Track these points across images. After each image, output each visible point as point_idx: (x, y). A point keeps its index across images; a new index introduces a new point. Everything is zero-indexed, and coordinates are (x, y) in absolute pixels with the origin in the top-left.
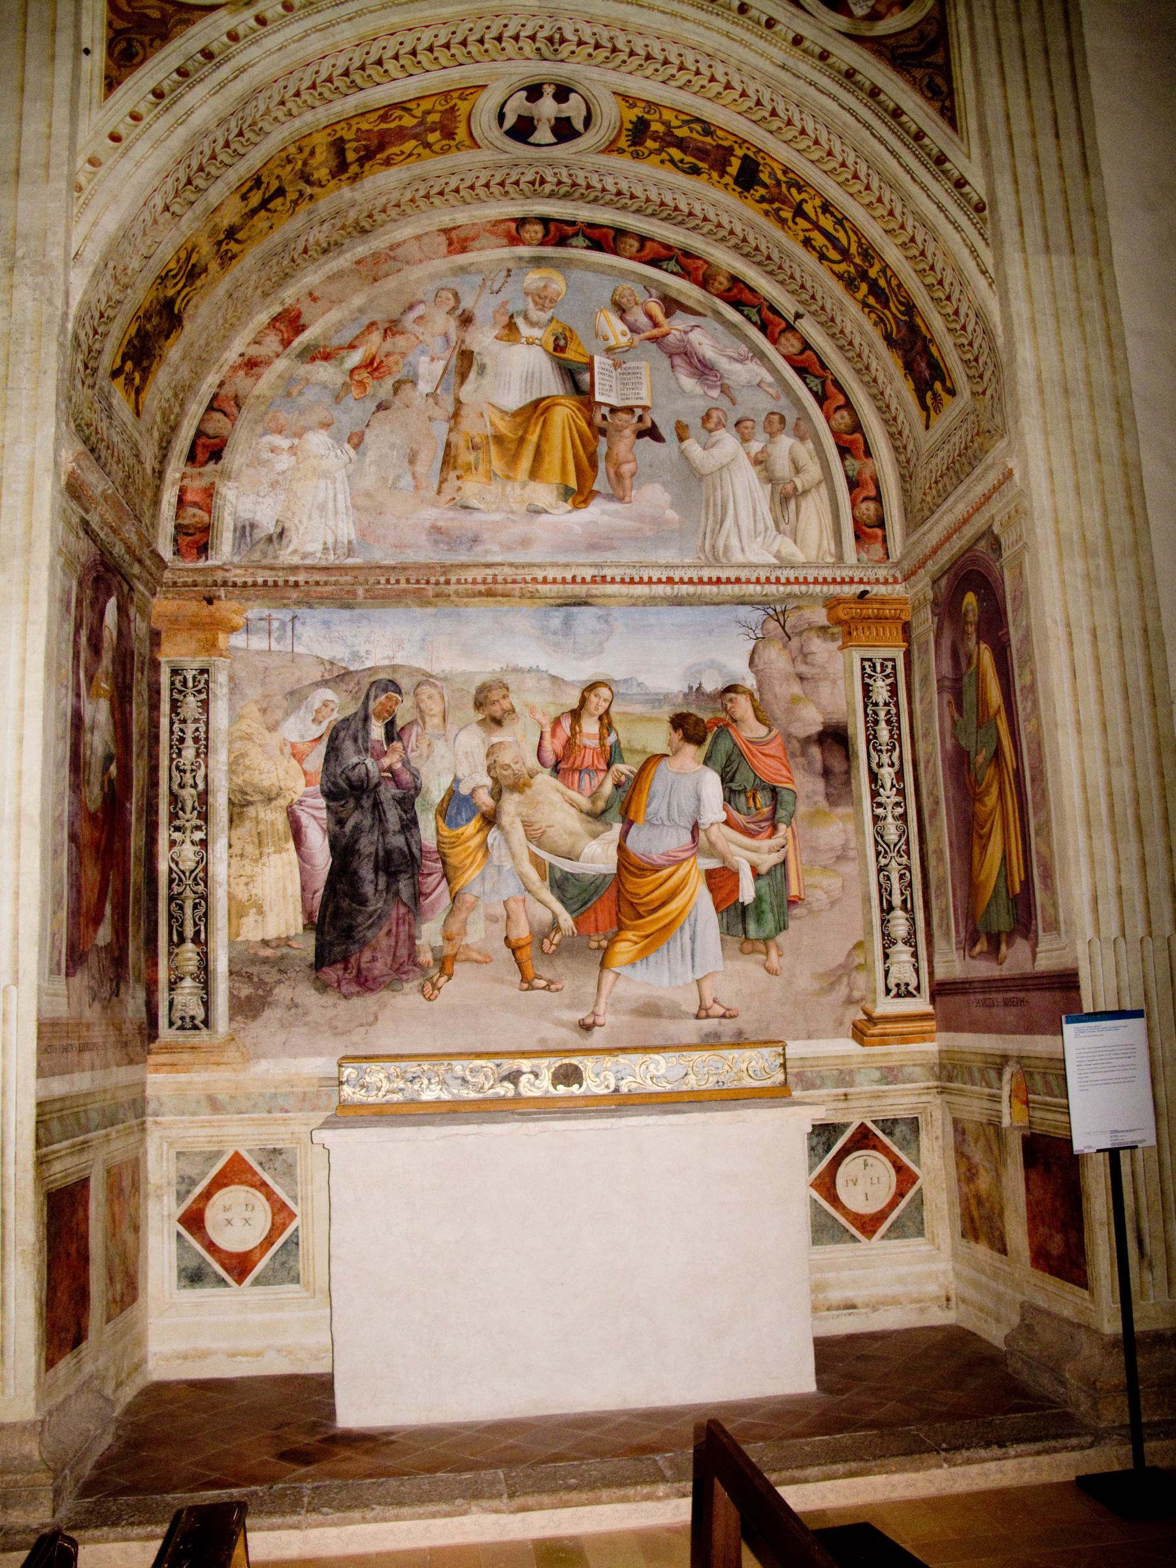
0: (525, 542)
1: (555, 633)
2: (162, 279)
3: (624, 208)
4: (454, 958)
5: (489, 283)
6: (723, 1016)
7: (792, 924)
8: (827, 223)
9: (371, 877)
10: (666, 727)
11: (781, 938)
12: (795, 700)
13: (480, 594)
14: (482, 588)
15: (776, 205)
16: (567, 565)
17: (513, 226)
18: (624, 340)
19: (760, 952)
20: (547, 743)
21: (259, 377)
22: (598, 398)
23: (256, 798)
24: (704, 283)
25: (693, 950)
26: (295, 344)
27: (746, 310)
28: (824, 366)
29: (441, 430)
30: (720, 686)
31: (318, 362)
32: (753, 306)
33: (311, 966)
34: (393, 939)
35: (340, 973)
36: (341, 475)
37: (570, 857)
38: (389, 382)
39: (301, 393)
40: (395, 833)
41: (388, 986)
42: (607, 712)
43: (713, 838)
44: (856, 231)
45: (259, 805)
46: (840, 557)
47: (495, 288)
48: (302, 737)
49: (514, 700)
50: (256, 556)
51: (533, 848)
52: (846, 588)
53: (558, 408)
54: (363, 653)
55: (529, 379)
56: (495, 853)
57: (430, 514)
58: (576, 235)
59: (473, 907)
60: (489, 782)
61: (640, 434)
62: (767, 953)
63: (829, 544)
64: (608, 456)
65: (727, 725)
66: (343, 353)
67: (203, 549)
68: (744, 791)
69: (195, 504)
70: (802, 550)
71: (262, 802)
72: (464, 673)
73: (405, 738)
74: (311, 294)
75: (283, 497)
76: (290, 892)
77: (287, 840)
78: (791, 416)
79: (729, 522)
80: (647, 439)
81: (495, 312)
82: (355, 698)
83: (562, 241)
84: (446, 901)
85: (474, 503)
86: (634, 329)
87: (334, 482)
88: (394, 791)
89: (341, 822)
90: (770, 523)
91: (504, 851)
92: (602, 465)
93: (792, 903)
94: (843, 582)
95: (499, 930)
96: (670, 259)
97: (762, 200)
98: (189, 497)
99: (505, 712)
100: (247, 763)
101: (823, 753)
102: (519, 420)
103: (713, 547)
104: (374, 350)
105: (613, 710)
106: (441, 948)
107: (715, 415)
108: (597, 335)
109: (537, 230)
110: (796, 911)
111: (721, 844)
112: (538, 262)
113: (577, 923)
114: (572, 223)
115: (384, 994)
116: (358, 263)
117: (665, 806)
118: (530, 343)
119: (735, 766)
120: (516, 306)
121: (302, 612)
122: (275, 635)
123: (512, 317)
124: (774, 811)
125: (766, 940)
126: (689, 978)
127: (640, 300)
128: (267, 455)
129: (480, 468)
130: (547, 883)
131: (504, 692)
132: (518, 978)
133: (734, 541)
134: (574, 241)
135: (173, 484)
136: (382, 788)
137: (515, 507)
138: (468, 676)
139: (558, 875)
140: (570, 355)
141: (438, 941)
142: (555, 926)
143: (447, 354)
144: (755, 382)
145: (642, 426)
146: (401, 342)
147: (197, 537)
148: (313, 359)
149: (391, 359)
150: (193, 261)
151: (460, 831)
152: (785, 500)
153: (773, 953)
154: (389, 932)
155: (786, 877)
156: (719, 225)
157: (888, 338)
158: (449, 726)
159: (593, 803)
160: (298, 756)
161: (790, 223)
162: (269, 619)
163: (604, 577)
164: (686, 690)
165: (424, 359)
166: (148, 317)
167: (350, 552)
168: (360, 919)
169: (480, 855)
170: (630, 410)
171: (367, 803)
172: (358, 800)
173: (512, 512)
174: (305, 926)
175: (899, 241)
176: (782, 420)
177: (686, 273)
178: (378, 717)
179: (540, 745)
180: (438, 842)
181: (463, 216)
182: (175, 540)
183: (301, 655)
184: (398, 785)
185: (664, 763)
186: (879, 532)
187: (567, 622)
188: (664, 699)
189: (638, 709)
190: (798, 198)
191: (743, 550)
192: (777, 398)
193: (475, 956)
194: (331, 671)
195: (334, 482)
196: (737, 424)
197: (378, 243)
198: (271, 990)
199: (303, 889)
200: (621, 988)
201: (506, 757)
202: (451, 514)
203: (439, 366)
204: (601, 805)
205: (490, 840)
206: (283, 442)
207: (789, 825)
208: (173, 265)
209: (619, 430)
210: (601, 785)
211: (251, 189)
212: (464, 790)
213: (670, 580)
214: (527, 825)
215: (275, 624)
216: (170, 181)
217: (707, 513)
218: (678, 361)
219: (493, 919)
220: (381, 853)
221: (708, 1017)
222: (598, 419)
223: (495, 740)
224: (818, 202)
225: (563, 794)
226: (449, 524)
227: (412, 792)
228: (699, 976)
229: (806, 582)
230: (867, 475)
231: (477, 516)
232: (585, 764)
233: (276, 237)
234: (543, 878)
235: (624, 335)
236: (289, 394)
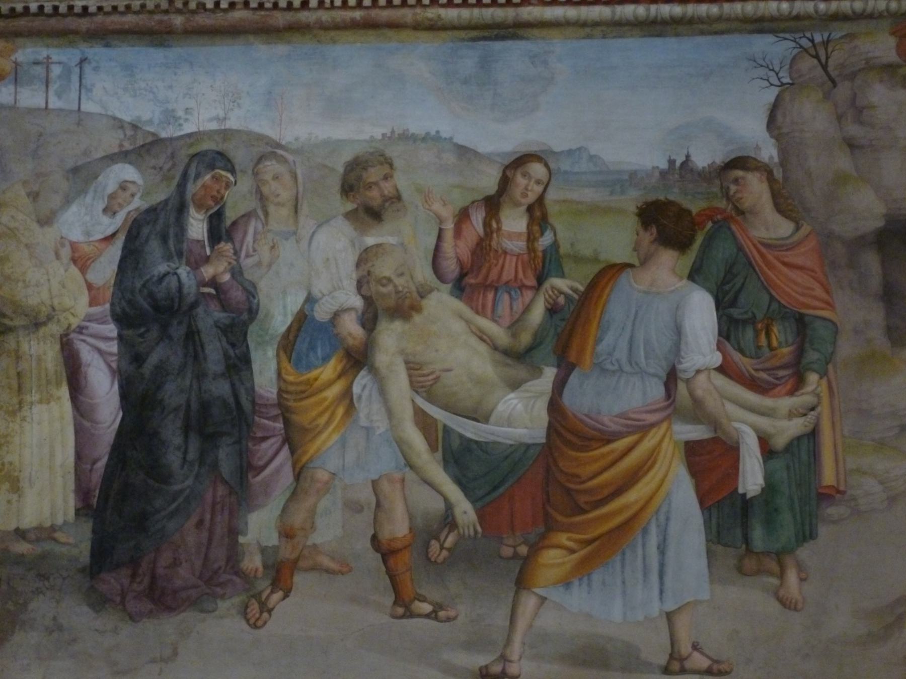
1: (465, 82)
4: (294, 565)
6: (709, 672)
7: (823, 531)
9: (178, 440)
10: (632, 222)
11: (804, 553)
12: (841, 179)
14: (358, 14)
19: (771, 574)
20: (448, 245)
23: (18, 322)
25: (662, 566)
30: (719, 159)
33: (82, 570)
34: (205, 534)
35: (126, 582)
37: (479, 415)
40: (216, 377)
41: (195, 603)
42: (541, 199)
43: (699, 393)
45: (21, 333)
48: (88, 234)
49: (401, 182)
51: (421, 403)
54: (180, 113)
56: (363, 410)
59: (327, 488)
60: (357, 302)
62: (782, 575)
65: (728, 219)
68: (753, 321)
71: (25, 327)
72: (327, 143)
73: (238, 236)
76: (59, 460)
77: (58, 385)
82: (167, 178)
84: (287, 478)
88: (219, 315)
89: (138, 359)
91: (377, 406)
93: (827, 496)
95: (363, 523)
99: (386, 199)
100: (8, 271)
101: (883, 263)
105: (552, 195)
106: (276, 549)
110: (832, 511)
111: (712, 403)
113: (481, 515)
115: (189, 616)
117: (623, 345)
119: (738, 282)
121: (96, 52)
122: (53, 88)
124: (800, 353)
125: (780, 556)
126: (655, 609)
130: (439, 455)
131: (386, 169)
132: (389, 599)
136: (200, 310)
138: (333, 146)
139: (456, 443)
141: (272, 539)
142: (448, 520)
151: (314, 373)
153: (792, 576)
154: (200, 524)
155: (815, 455)
158: (302, 219)
159: (514, 336)
160: (81, 261)
162: (47, 63)
164: (664, 165)
168: (158, 503)
169: (341, 411)
171: (178, 331)
172: (165, 327)
174: (78, 512)
178: (199, 207)
179: (437, 249)
180: (280, 391)
183: (89, 114)
184: (224, 307)
185: (625, 278)
187: (485, 64)
188: (633, 178)
189: (589, 195)
193: (326, 562)
194: (133, 138)
198: (25, 604)
199: (79, 456)
200: (548, 620)
201: (385, 268)
204: (526, 339)
205: (356, 389)
207: (823, 374)
210: (527, 309)
212: (322, 313)
214: (413, 367)
215: (56, 70)
219: (353, 507)
220: (194, 406)
221: (683, 671)
223: (370, 241)
225: (468, 322)
227: (245, 316)
228: (670, 606)
232: (505, 278)
234: (433, 448)
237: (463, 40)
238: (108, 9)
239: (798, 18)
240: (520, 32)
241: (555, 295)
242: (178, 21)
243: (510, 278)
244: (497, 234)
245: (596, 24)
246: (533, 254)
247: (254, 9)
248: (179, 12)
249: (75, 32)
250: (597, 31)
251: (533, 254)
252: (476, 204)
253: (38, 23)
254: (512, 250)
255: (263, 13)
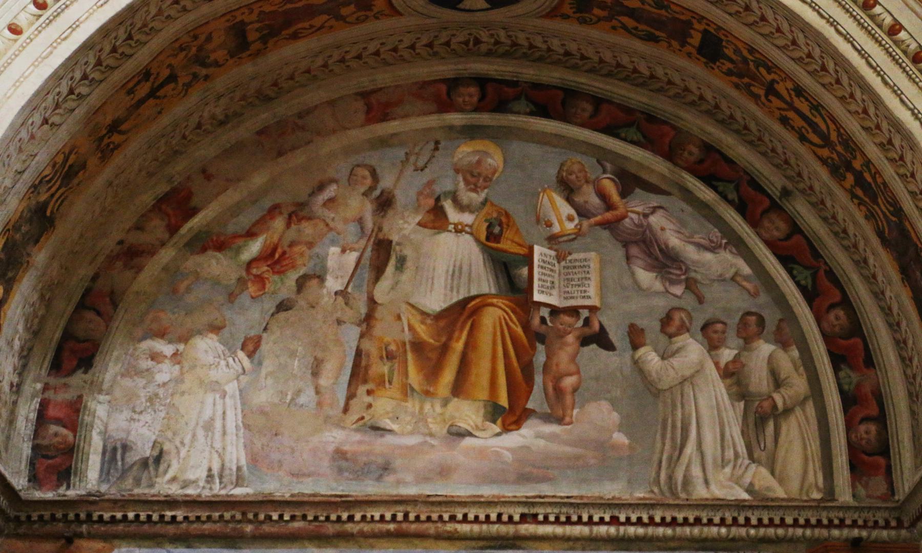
0: (444, 472)
2: (34, 188)
3: (575, 67)
5: (412, 159)
8: (804, 107)
13: (388, 535)
14: (392, 527)
15: (746, 80)
16: (490, 503)
17: (443, 88)
18: (570, 226)
21: (140, 269)
22: (537, 297)
24: (669, 155)
26: (184, 230)
27: (721, 186)
28: (816, 254)
29: (352, 334)
31: (210, 253)
32: (730, 182)
36: (232, 388)
38: (292, 277)
39: (188, 290)
44: (834, 120)
46: (830, 492)
47: (420, 164)
50: (129, 483)
52: (836, 533)
53: (491, 309)
55: (457, 273)
57: (335, 437)
58: (517, 98)
61: (585, 341)
63: (816, 477)
64: (546, 368)
66: (240, 242)
67: (65, 475)
69: (58, 421)
70: (781, 481)
74: (204, 171)
75: (163, 414)
78: (772, 316)
79: (690, 448)
80: (594, 346)
81: (420, 194)
83: (501, 107)
85: (387, 423)
86: (583, 212)
87: (224, 396)
90: (742, 449)
92: (538, 379)
94: (831, 525)
96: (629, 125)
97: (729, 73)
98: (52, 412)
102: (442, 323)
103: (670, 478)
104: (275, 239)
107: (677, 317)
108: (538, 221)
109: (471, 93)
112: (471, 132)
114: (514, 84)
116: (260, 133)
118: (459, 230)
120: (446, 185)
123: (438, 199)
127: (592, 177)
128: (146, 364)
129: (395, 380)
133: (696, 471)
134: (516, 106)
135: (33, 397)
137: (434, 427)
140: (505, 245)
143: (363, 242)
144: (729, 275)
145: (587, 331)
146: (308, 229)
147: (58, 460)
148: (204, 250)
149: (296, 249)
150: (70, 162)
152: (761, 421)
156: (686, 89)
157: (880, 234)
161: (763, 98)
163: (535, 516)
165: (334, 250)
166: (16, 228)
167: (239, 481)
170: (574, 311)
173: (431, 435)
175: (878, 140)
176: (761, 321)
177: (647, 143)
181: (384, 78)
182: (32, 463)
186: (881, 461)
190: (769, 78)
191: (706, 482)
192: (755, 295)
195: (224, 396)
196: (704, 328)
197: (283, 109)
202: (358, 437)
203: (352, 257)
206: (167, 349)
208: (47, 172)
209: (561, 335)
211: (139, 82)
213: (614, 520)
216: (50, 97)
217: (663, 437)
218: (634, 250)
222: (536, 321)
224: (790, 85)
226: (355, 448)
229: (783, 523)
230: (867, 389)
231: (389, 439)
233: (165, 120)
235: (570, 219)
236: (175, 291)
237: (474, 548)
238: (192, 518)
239: (733, 539)
240: (518, 543)
242: (249, 528)
245: (577, 539)
247: (310, 521)
248: (250, 522)
249: (163, 536)
250: (578, 545)
253: (133, 528)
255: (317, 524)
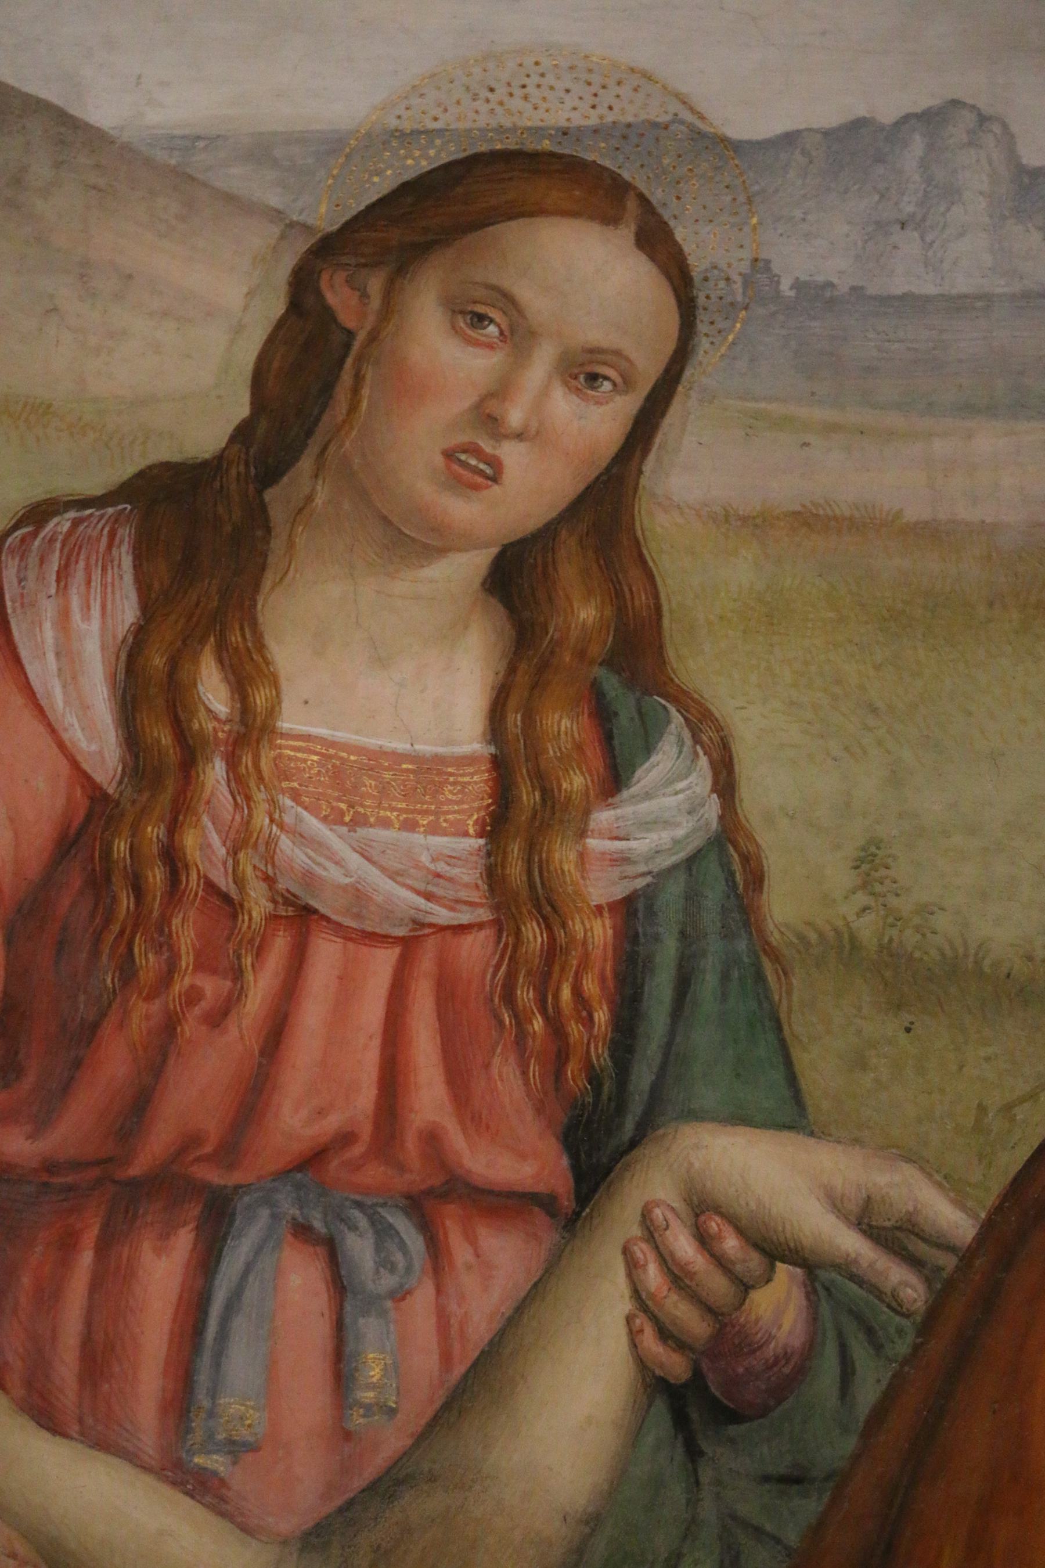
241: (721, 1262)
243: (333, 1123)
244: (232, 763)
246: (534, 935)
251: (534, 935)
252: (62, 524)
254: (358, 895)
